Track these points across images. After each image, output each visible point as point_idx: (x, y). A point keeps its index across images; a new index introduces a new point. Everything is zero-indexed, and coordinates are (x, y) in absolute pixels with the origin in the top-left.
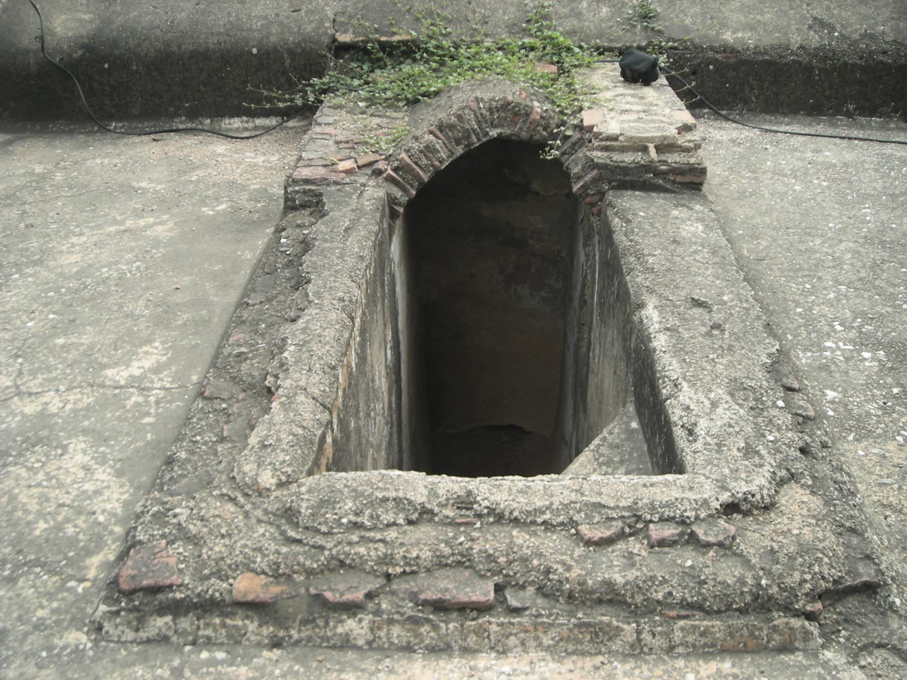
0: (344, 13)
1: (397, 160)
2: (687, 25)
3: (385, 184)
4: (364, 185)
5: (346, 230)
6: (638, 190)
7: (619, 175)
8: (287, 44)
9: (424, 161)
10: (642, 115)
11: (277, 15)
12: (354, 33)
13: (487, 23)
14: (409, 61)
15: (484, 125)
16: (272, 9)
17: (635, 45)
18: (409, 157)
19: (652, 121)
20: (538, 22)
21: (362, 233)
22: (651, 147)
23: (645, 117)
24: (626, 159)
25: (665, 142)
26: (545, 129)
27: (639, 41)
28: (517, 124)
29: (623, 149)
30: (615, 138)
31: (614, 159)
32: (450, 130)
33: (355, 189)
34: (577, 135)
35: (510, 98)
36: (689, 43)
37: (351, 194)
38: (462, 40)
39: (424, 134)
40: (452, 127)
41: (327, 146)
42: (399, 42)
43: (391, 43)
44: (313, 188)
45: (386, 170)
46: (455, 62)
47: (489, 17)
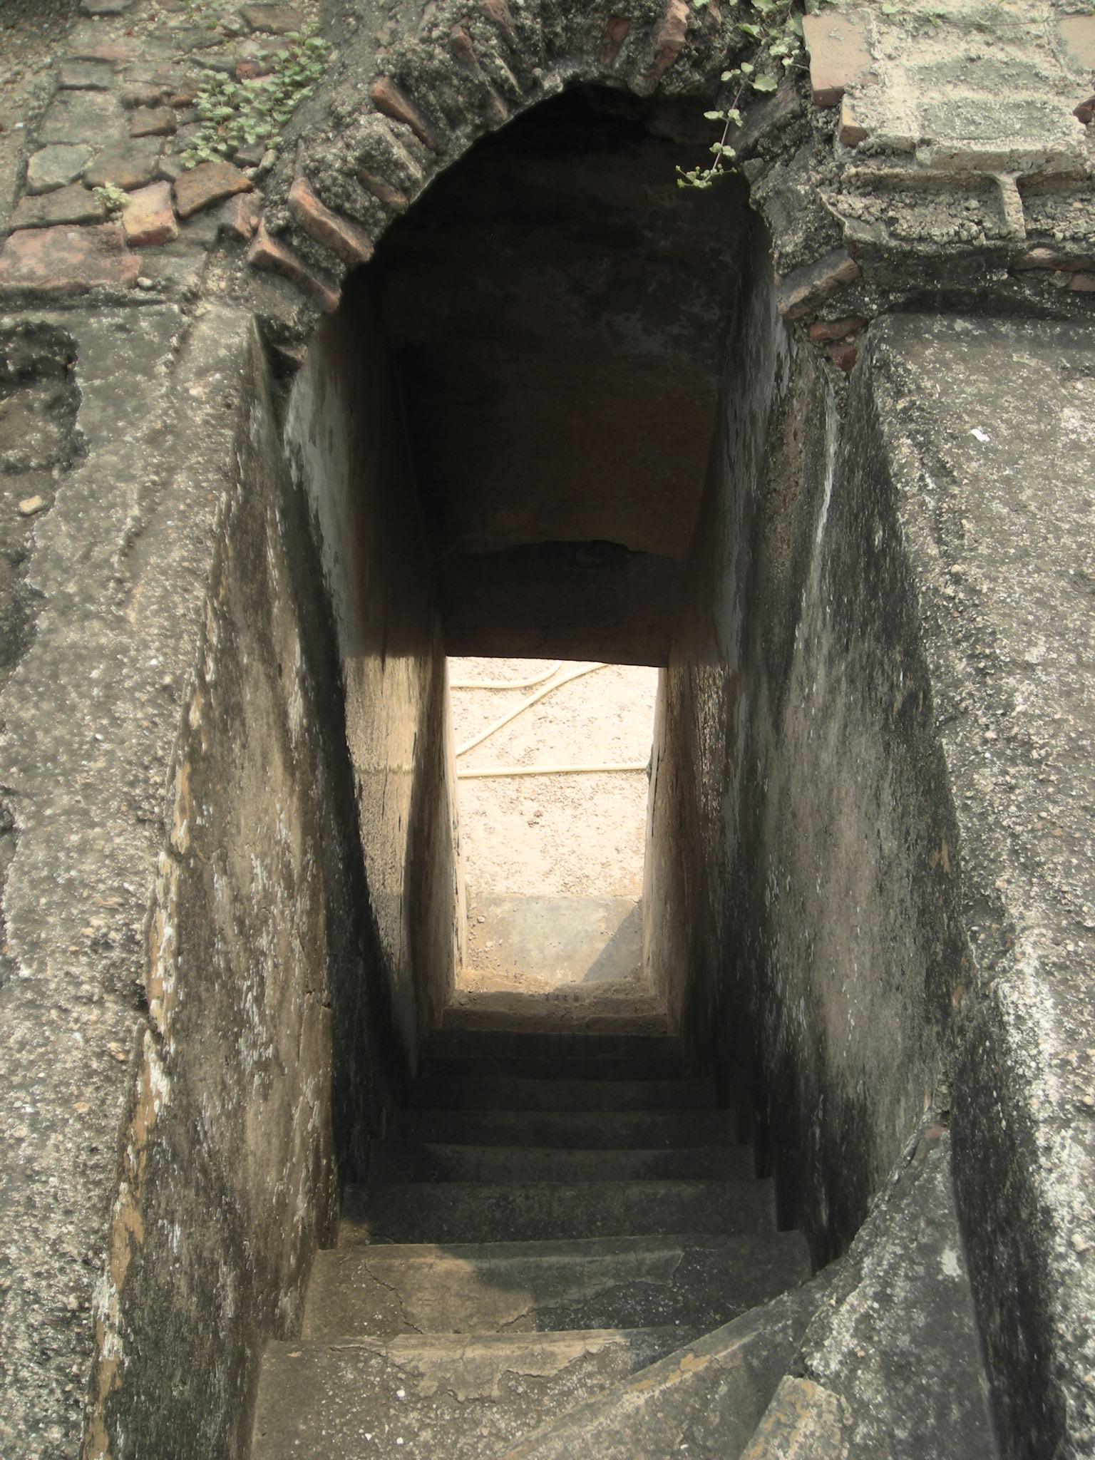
1: (284, 202)
3: (254, 285)
4: (192, 297)
5: (128, 550)
6: (962, 314)
7: (914, 275)
9: (361, 200)
15: (528, 59)
18: (317, 193)
21: (176, 555)
22: (1008, 181)
24: (935, 232)
25: (1050, 170)
26: (697, 64)
28: (616, 46)
29: (923, 190)
30: (906, 152)
31: (902, 228)
32: (432, 87)
33: (165, 325)
34: (787, 104)
37: (155, 352)
39: (356, 109)
40: (436, 79)
41: (97, 119)
44: (52, 318)
45: (255, 231)
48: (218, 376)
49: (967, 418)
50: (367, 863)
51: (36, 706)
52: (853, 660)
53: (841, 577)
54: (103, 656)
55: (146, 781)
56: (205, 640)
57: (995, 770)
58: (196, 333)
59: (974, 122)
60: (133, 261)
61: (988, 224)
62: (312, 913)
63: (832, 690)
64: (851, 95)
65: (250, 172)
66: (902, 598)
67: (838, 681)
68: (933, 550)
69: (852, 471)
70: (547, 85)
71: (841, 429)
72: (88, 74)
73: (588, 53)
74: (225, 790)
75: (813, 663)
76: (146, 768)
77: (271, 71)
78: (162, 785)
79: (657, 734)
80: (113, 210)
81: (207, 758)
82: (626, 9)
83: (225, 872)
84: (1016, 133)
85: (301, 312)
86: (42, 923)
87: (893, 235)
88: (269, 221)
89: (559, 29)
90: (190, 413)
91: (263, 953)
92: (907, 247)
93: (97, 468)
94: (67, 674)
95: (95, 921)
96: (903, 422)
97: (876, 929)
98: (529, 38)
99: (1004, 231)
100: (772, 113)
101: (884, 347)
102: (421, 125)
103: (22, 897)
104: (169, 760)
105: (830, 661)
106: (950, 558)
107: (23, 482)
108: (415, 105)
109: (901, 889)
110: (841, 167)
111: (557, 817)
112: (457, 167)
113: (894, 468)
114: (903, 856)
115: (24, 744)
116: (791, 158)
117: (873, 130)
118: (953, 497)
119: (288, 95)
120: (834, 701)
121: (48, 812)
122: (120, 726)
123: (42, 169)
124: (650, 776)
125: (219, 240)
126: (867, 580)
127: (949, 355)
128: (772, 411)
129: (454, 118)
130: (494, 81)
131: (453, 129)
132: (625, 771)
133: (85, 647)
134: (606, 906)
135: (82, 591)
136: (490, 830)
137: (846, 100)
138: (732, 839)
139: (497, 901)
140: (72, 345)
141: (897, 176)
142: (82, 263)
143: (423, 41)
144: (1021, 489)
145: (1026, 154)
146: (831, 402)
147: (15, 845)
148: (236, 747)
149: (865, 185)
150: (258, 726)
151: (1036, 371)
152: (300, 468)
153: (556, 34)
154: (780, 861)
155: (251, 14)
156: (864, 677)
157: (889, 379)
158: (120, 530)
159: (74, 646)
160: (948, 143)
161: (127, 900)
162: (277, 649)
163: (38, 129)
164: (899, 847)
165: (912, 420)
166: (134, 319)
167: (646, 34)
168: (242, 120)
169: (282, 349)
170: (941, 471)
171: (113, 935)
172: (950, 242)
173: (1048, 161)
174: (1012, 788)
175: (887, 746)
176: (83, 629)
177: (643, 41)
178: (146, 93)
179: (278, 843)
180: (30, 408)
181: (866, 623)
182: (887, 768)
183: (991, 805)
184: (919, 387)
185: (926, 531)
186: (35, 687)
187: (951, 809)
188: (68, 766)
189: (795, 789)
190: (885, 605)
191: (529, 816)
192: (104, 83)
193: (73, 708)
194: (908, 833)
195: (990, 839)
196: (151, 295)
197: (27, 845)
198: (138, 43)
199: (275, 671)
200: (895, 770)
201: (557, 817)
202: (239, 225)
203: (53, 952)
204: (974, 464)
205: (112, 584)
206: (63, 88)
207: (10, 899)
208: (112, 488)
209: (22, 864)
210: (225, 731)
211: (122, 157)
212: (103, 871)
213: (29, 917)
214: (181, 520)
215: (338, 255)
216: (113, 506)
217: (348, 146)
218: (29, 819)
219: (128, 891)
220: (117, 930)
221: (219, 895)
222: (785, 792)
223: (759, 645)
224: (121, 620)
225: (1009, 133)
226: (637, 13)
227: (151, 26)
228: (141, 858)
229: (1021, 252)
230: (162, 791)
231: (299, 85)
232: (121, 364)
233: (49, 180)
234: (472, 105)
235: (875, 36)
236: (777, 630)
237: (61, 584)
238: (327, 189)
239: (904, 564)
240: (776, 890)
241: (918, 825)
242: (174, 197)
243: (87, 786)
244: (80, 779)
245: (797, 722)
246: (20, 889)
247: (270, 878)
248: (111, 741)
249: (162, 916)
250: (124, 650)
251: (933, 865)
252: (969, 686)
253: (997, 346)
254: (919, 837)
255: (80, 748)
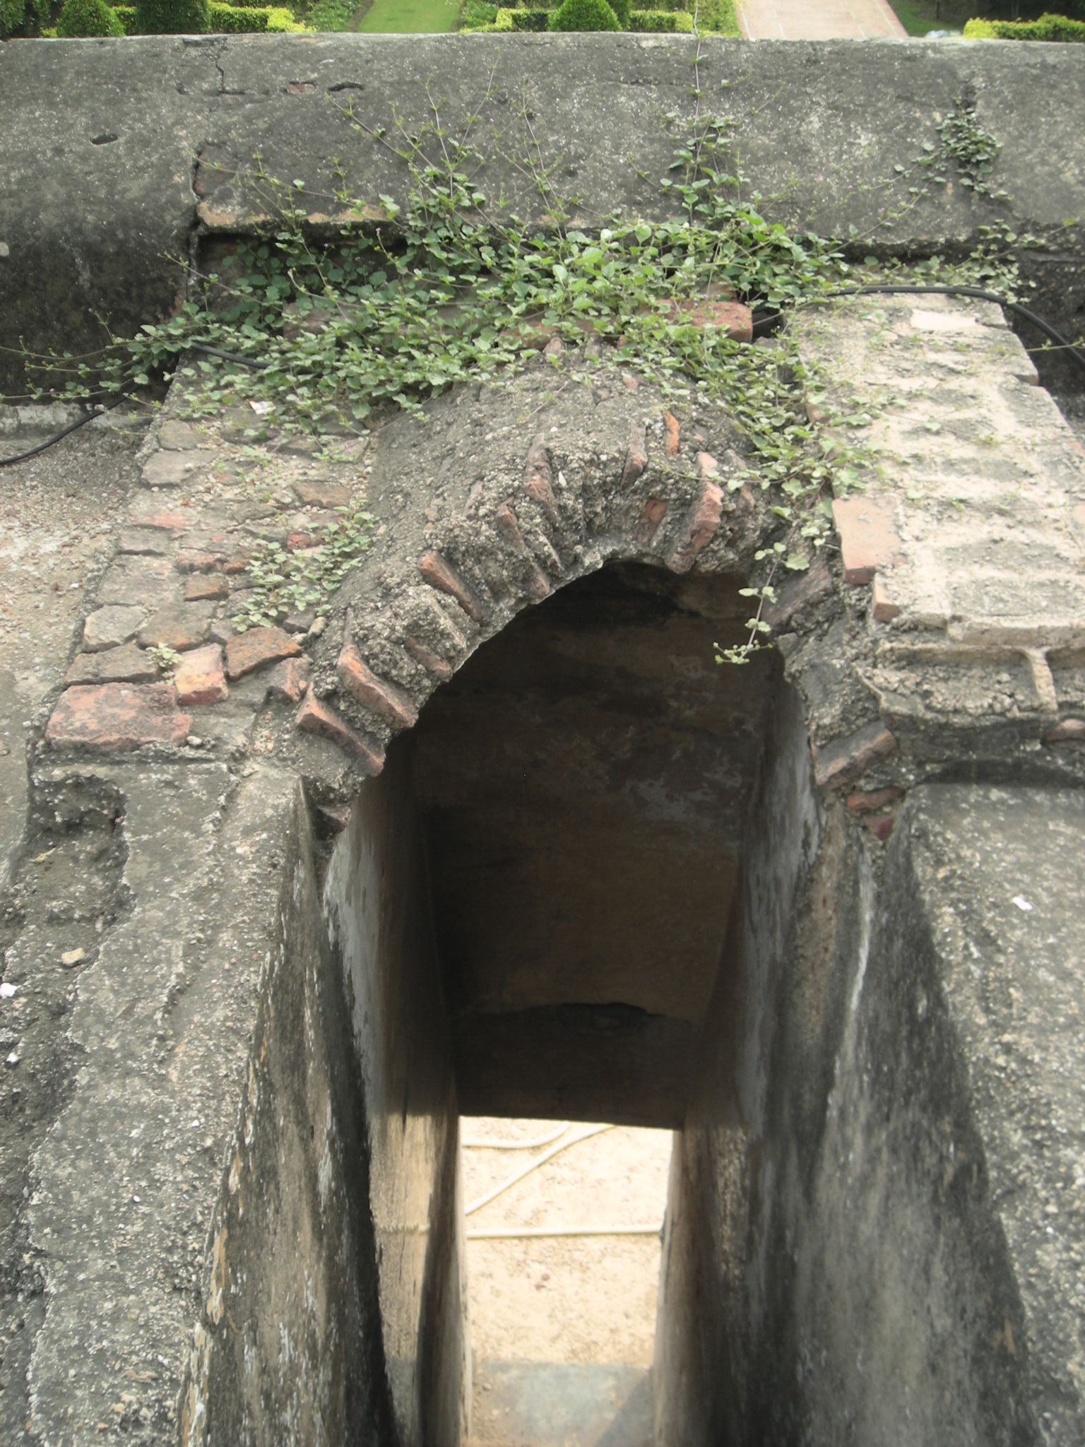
0: (220, 146)
1: (333, 667)
2: (1067, 186)
3: (301, 746)
4: (240, 757)
6: (997, 784)
8: (79, 231)
9: (407, 667)
10: (997, 528)
11: (59, 151)
12: (245, 202)
13: (572, 174)
14: (379, 277)
15: (570, 537)
16: (46, 133)
17: (942, 240)
18: (366, 659)
19: (1033, 556)
20: (699, 175)
21: (220, 1014)
22: (1037, 656)
23: (1010, 535)
24: (970, 704)
26: (731, 544)
27: (953, 227)
28: (654, 526)
29: (956, 663)
30: (938, 628)
31: (937, 701)
32: (478, 561)
34: (819, 582)
35: (639, 456)
36: (1073, 237)
37: (203, 809)
38: (511, 224)
40: (482, 553)
41: (153, 583)
42: (355, 226)
43: (336, 228)
44: (101, 772)
45: (303, 694)
46: (496, 290)
47: (578, 157)
48: (264, 836)
49: (1007, 886)
50: (385, 1329)
51: (73, 1164)
52: (896, 1129)
53: (879, 1046)
54: (143, 1115)
55: (184, 1247)
56: (246, 1102)
57: (1059, 1245)
58: (244, 793)
59: (1002, 600)
60: (183, 719)
61: (1020, 697)
62: (333, 1384)
63: (872, 1159)
64: (883, 574)
65: (299, 637)
66: (951, 1067)
67: (878, 1150)
68: (981, 1020)
69: (890, 939)
70: (587, 562)
71: (878, 897)
72: (146, 541)
73: (626, 532)
74: (258, 1256)
75: (849, 1131)
76: (185, 1234)
77: (321, 542)
78: (200, 1252)
79: (671, 1197)
80: (164, 670)
81: (242, 1224)
82: (663, 491)
83: (254, 1342)
84: (1043, 610)
85: (346, 775)
86: (70, 1396)
87: (929, 708)
88: (317, 684)
89: (599, 510)
90: (236, 872)
91: (287, 1429)
92: (942, 719)
93: (142, 922)
94: (108, 1131)
95: (126, 1397)
96: (945, 890)
97: (929, 1411)
98: (571, 517)
99: (1036, 704)
100: (804, 590)
101: (922, 817)
102: (466, 597)
103: (50, 1368)
104: (208, 1226)
105: (869, 1130)
106: (999, 1027)
107: (65, 933)
108: (461, 578)
109: (958, 1369)
110: (875, 642)
111: (564, 1281)
112: (498, 637)
113: (937, 938)
114: (959, 1333)
115: (58, 1203)
116: (825, 633)
117: (906, 607)
118: (1000, 965)
119: (337, 565)
120: (874, 1170)
121: (82, 1277)
122: (159, 1189)
123: (98, 628)
124: (662, 1239)
125: (267, 702)
126: (910, 1049)
127: (986, 824)
128: (799, 878)
129: (498, 591)
130: (537, 556)
131: (497, 601)
132: (634, 1234)
133: (126, 1106)
134: (616, 1374)
135: (123, 1047)
136: (497, 1293)
137: (878, 579)
138: (756, 1310)
139: (504, 1367)
140: (120, 799)
141: (930, 651)
142: (134, 719)
143: (470, 518)
144: (1067, 957)
145: (1054, 630)
146: (865, 870)
147: (44, 1311)
148: (270, 1212)
149: (899, 659)
150: (290, 1188)
151: (1073, 839)
152: (337, 928)
153: (596, 514)
154: (813, 1334)
155: (302, 489)
156: (909, 1148)
157: (928, 847)
158: (164, 987)
159: (113, 1102)
160: (979, 620)
161: (161, 1374)
162: (310, 1110)
163: (96, 590)
164: (954, 1325)
165: (953, 889)
166: (183, 776)
167: (683, 515)
168: (293, 588)
169: (326, 810)
170: (985, 940)
171: (144, 1411)
172: (984, 715)
173: (1075, 636)
174: (1077, 1266)
175: (937, 1220)
176: (124, 1086)
177: (680, 521)
178: (201, 560)
179: (304, 1311)
180: (75, 859)
181: (909, 1093)
182: (936, 1243)
183: (1057, 1282)
184: (959, 858)
185: (973, 1001)
186: (72, 1144)
187: (1014, 1287)
188: (104, 1228)
189: (830, 1259)
190: (930, 1073)
191: (537, 1279)
192: (161, 549)
193: (111, 1168)
194: (964, 1311)
195: (1058, 1318)
196: (200, 753)
197: (57, 1311)
198: (194, 513)
199: (308, 1133)
200: (946, 1245)
201: (564, 1281)
202: (287, 687)
203: (80, 1429)
204: (1018, 933)
205: (154, 1042)
206: (121, 552)
207: (36, 1370)
208: (157, 944)
209: (52, 1332)
210: (260, 1195)
211: (176, 619)
212: (136, 1342)
213: (55, 1389)
214: (225, 978)
215: (383, 721)
216: (156, 962)
217: (396, 615)
218: (61, 1283)
219: (162, 1365)
220: (148, 1407)
221: (248, 1367)
222: (818, 1263)
223: (787, 1112)
224: (164, 1078)
225: (1036, 610)
226: (673, 496)
227: (207, 498)
228: (176, 1329)
229: (1053, 724)
230: (200, 1259)
231: (348, 556)
232: (169, 819)
233: (105, 639)
234: (515, 579)
235: (902, 520)
236: (807, 1097)
237: (102, 1039)
238: (375, 656)
239: (952, 1032)
240: (810, 1365)
241: (976, 1303)
242: (224, 658)
243: (122, 1250)
244: (116, 1243)
245: (830, 1191)
246: (48, 1359)
247: (295, 1348)
248: (150, 1204)
249: (195, 1391)
250: (166, 1110)
251: (995, 1344)
252: (1026, 1158)
253: (1032, 815)
254: (977, 1315)
255: (117, 1210)
